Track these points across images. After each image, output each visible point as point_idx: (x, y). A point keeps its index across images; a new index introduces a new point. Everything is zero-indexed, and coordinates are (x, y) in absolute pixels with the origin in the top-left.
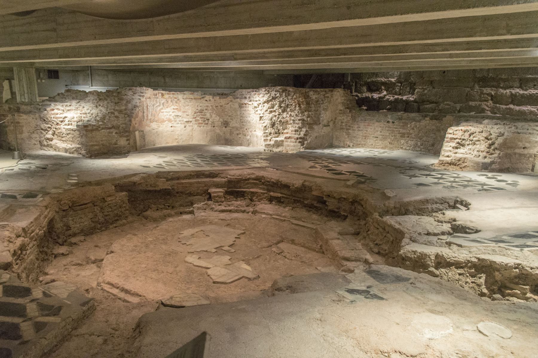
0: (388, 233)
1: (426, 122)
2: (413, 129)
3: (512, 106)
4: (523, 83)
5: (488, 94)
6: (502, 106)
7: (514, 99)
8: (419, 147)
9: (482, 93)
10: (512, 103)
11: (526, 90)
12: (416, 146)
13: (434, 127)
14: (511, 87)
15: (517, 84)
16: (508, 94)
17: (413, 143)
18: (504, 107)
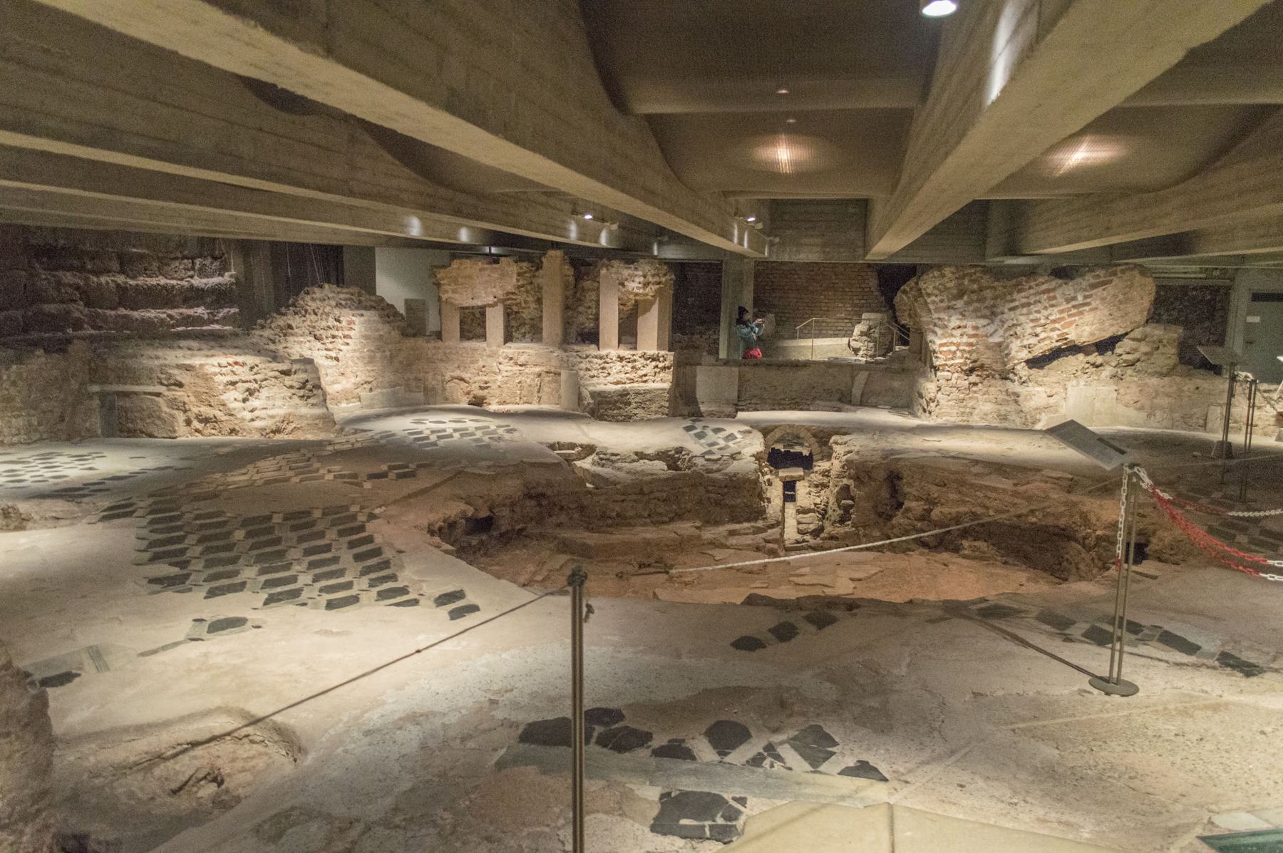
0: (652, 492)
1: (39, 360)
2: (14, 383)
3: (122, 311)
4: (127, 264)
5: (71, 286)
6: (108, 312)
7: (127, 297)
8: (36, 430)
9: (59, 283)
10: (121, 304)
11: (134, 278)
12: (30, 429)
13: (55, 372)
14: (108, 271)
15: (115, 265)
16: (112, 285)
17: (20, 422)
18: (113, 313)
